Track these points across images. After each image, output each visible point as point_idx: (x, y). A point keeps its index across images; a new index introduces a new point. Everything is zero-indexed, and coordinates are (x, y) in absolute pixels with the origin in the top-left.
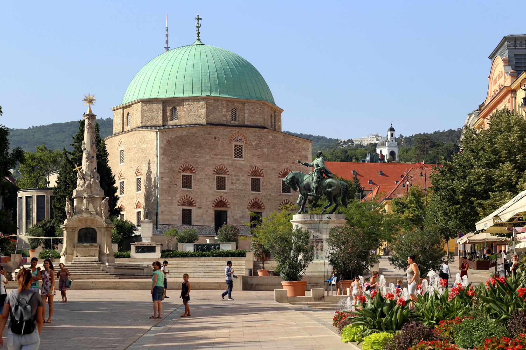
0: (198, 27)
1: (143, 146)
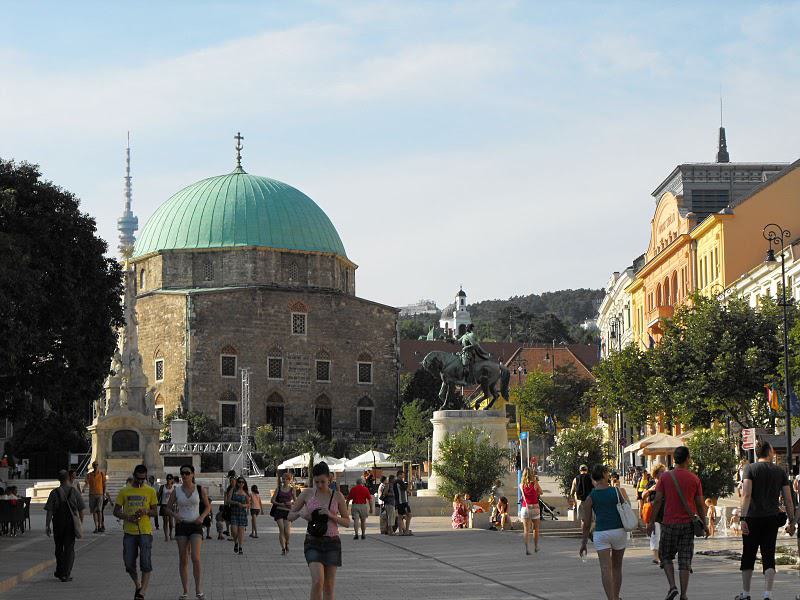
0: (239, 150)
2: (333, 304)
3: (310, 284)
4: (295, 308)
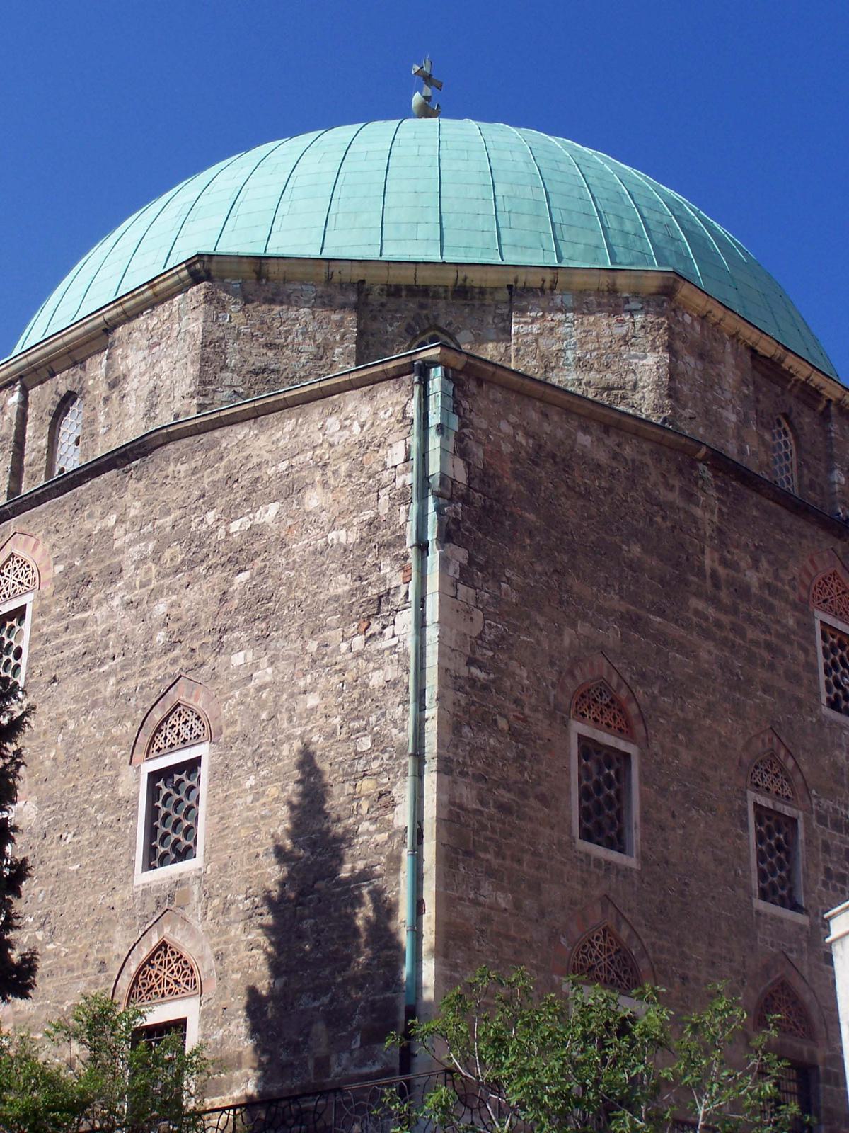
1: (235, 527)
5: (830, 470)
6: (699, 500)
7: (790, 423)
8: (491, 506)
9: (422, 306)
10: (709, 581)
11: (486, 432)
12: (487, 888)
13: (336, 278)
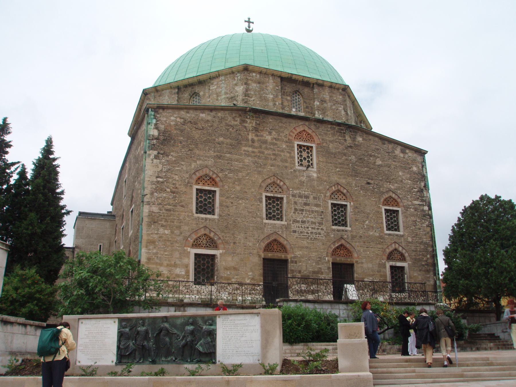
2: (347, 138)
3: (318, 115)
4: (299, 136)
5: (314, 102)
6: (247, 121)
7: (299, 92)
8: (167, 139)
9: (192, 88)
10: (250, 142)
11: (165, 121)
12: (161, 230)
13: (172, 87)
